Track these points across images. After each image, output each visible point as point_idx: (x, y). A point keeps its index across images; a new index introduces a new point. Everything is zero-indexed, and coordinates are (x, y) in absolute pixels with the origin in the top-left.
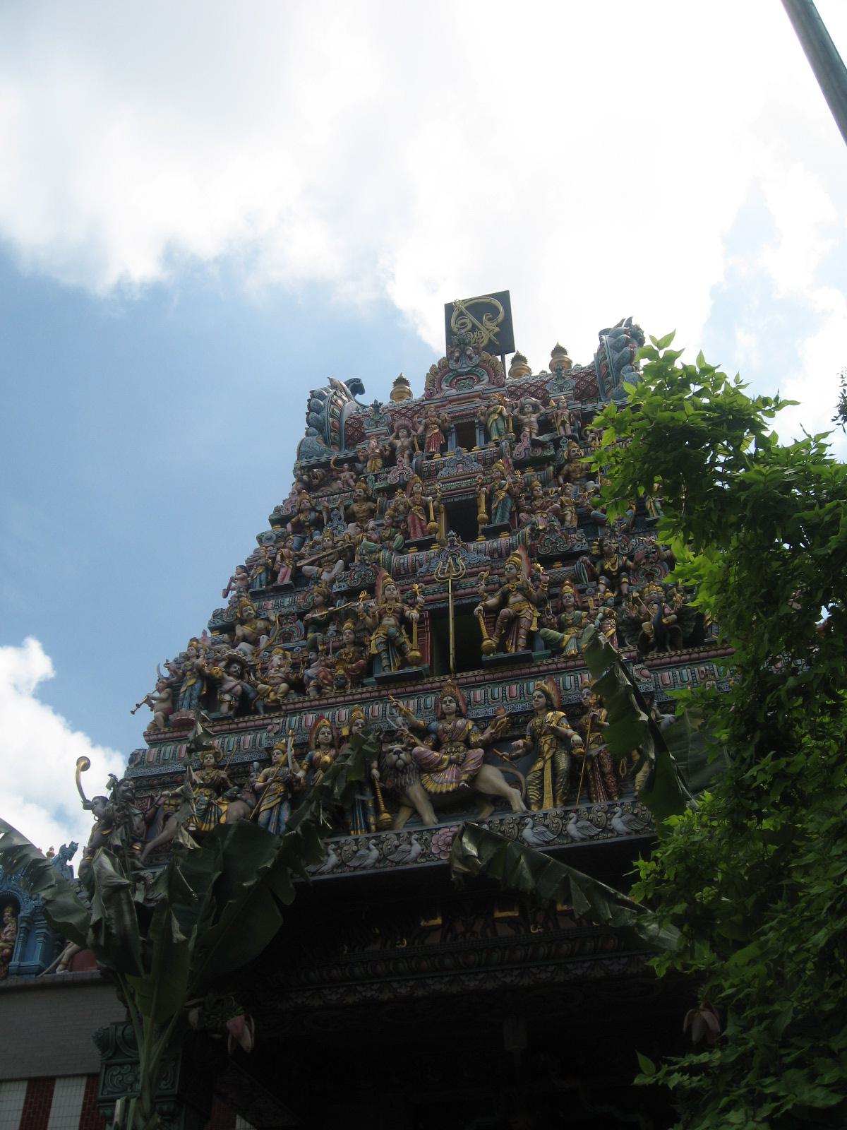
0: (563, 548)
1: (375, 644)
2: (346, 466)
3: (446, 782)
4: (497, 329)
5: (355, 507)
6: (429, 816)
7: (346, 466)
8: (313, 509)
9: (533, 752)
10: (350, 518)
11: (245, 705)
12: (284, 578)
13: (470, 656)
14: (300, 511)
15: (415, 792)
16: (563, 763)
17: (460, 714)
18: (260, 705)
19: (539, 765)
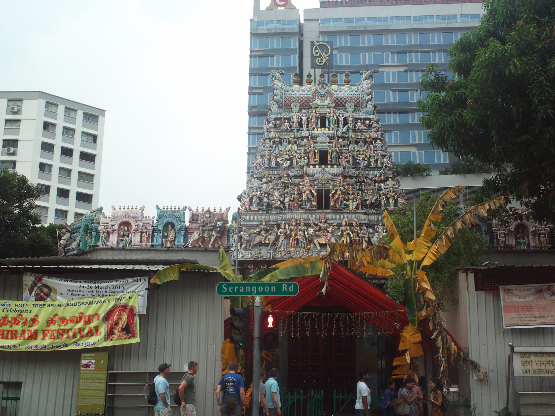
0: (350, 174)
1: (304, 197)
2: (286, 121)
3: (322, 241)
4: (328, 58)
5: (291, 139)
6: (319, 248)
7: (286, 121)
8: (279, 138)
9: (342, 235)
10: (289, 142)
11: (269, 205)
12: (273, 164)
13: (327, 207)
14: (275, 138)
15: (316, 241)
16: (348, 241)
17: (325, 222)
18: (273, 206)
19: (343, 239)
